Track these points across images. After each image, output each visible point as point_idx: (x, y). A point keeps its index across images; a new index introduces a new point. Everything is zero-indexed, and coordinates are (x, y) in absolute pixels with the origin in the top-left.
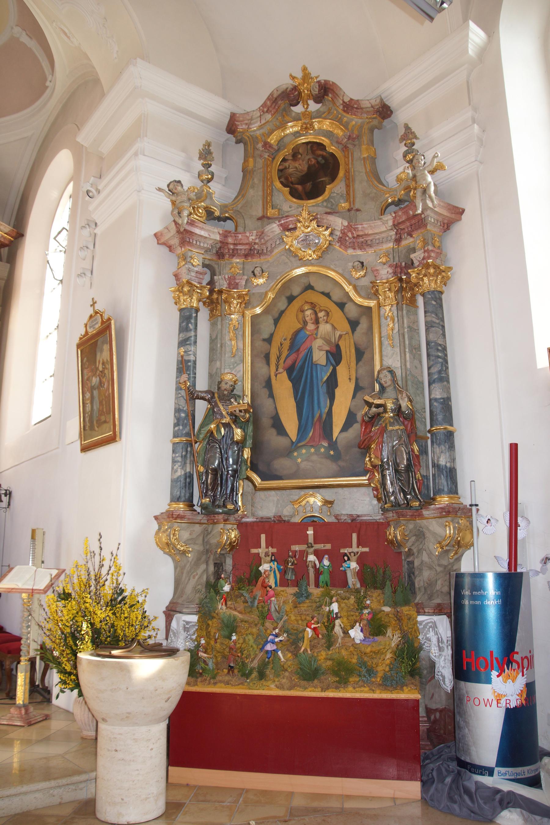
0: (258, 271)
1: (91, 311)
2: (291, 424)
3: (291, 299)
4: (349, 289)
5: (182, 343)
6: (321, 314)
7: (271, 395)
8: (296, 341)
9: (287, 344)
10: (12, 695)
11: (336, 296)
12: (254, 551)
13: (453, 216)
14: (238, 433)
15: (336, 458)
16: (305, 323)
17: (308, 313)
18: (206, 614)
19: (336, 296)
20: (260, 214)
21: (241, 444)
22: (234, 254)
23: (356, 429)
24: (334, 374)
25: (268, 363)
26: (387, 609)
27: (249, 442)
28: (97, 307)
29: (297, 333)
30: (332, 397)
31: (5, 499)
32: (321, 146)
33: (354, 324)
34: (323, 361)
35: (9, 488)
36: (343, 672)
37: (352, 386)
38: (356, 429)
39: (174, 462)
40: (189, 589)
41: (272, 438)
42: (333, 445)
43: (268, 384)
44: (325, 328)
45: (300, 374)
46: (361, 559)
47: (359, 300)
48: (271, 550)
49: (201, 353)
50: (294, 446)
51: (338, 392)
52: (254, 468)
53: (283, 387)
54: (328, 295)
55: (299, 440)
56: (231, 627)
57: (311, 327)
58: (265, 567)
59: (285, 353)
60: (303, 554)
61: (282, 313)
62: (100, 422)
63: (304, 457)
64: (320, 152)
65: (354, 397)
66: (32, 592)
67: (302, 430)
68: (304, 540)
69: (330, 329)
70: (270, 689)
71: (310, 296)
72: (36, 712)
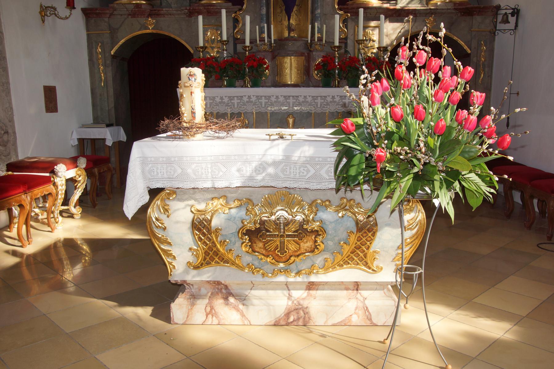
35: (517, 6)
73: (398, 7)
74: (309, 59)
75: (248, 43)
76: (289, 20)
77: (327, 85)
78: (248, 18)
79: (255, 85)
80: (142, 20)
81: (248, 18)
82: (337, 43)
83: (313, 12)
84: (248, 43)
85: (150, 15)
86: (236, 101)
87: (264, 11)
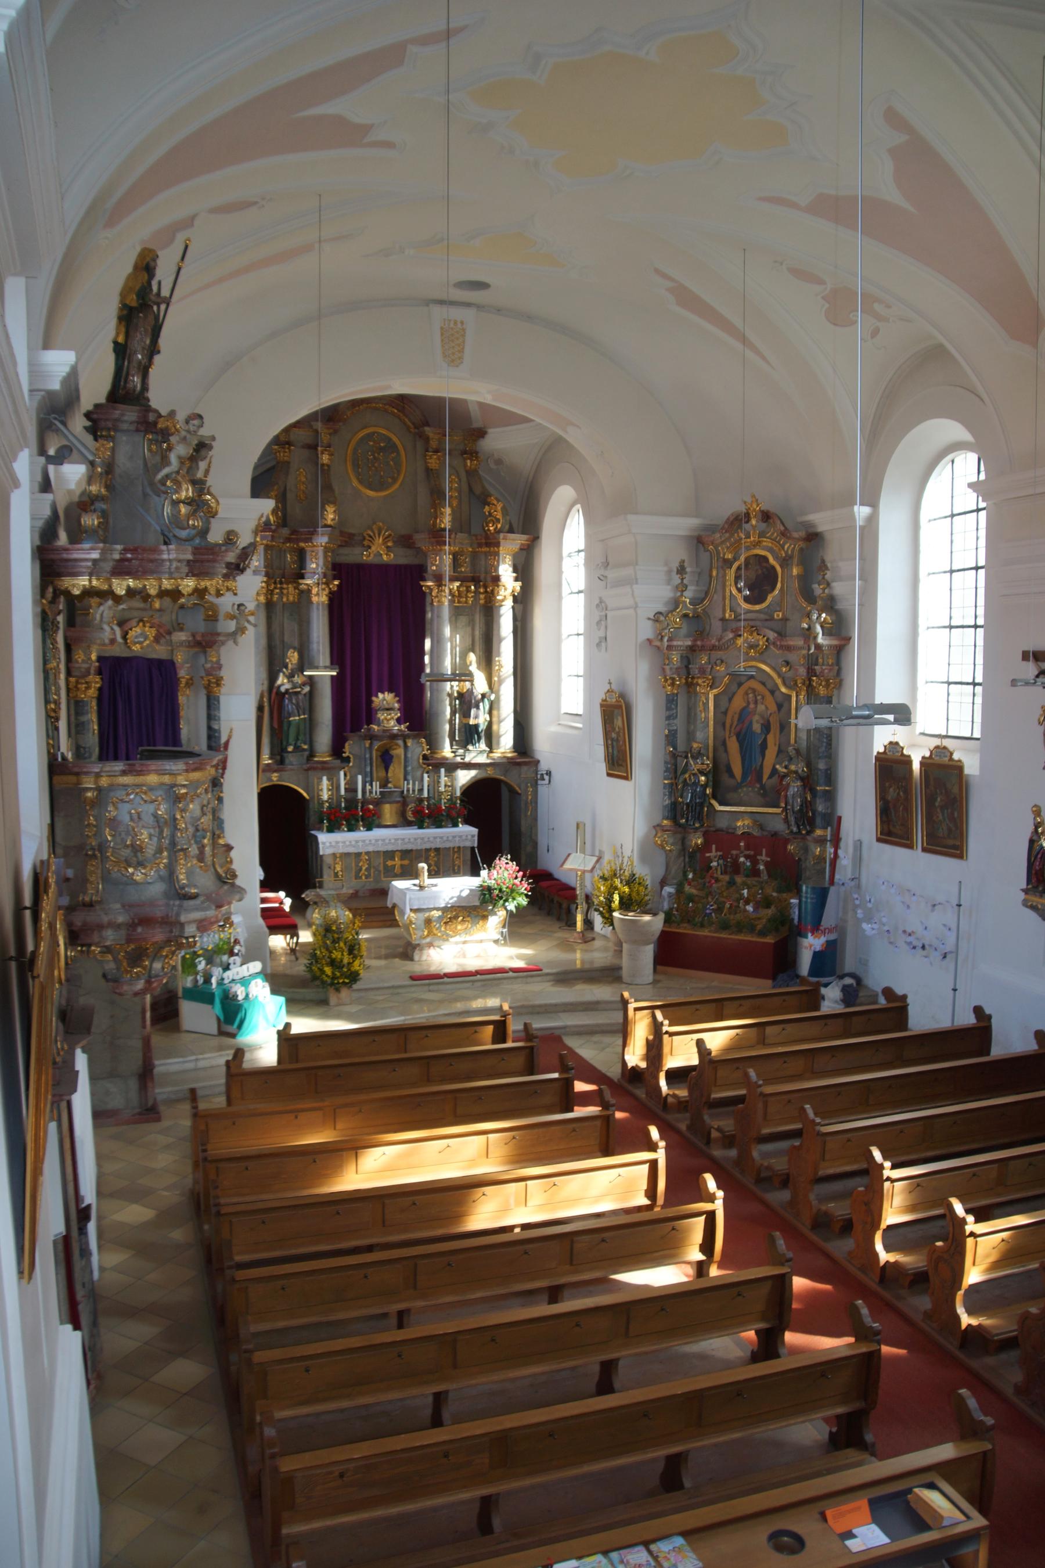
0: (718, 662)
1: (608, 687)
2: (737, 770)
3: (740, 685)
4: (779, 681)
5: (668, 718)
6: (759, 698)
7: (726, 751)
8: (744, 715)
9: (736, 717)
10: (574, 924)
11: (769, 685)
12: (708, 855)
13: (843, 642)
14: (703, 778)
15: (764, 795)
16: (749, 703)
17: (751, 695)
18: (680, 891)
19: (769, 685)
20: (721, 616)
21: (705, 786)
22: (703, 648)
23: (775, 779)
24: (765, 741)
25: (724, 729)
26: (775, 894)
27: (711, 783)
28: (613, 687)
29: (744, 709)
30: (763, 755)
31: (546, 777)
32: (765, 559)
33: (780, 706)
34: (759, 731)
36: (740, 928)
37: (776, 748)
38: (775, 779)
39: (665, 795)
40: (673, 871)
41: (725, 778)
42: (763, 787)
43: (724, 744)
44: (761, 708)
45: (744, 737)
46: (766, 864)
47: (783, 690)
48: (719, 853)
49: (679, 723)
50: (739, 786)
51: (767, 752)
52: (714, 797)
53: (733, 745)
54: (764, 684)
55: (742, 782)
56: (691, 898)
57: (752, 706)
58: (714, 864)
59: (735, 723)
60: (738, 857)
61: (734, 694)
62: (618, 762)
63: (744, 792)
64: (765, 564)
65: (777, 756)
66: (584, 872)
67: (745, 775)
68: (738, 848)
69: (767, 707)
70: (705, 932)
71: (753, 684)
72: (589, 935)
73: (467, 760)
74: (404, 803)
75: (360, 796)
76: (387, 772)
77: (421, 827)
78: (360, 777)
79: (369, 829)
80: (268, 774)
81: (360, 777)
82: (426, 795)
83: (405, 767)
84: (360, 796)
85: (275, 771)
86: (360, 844)
87: (368, 769)
